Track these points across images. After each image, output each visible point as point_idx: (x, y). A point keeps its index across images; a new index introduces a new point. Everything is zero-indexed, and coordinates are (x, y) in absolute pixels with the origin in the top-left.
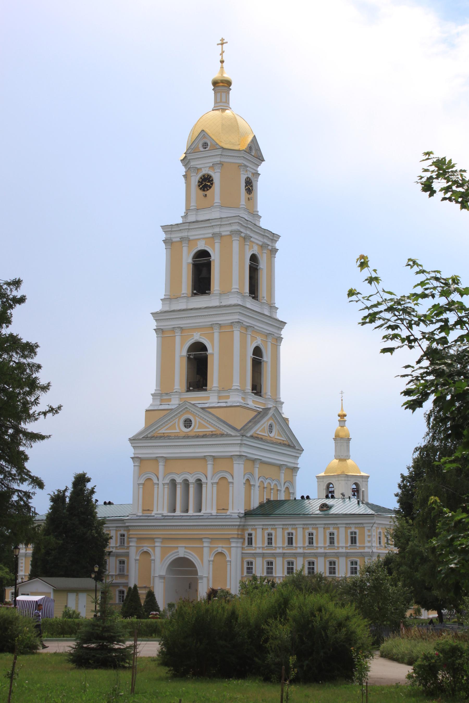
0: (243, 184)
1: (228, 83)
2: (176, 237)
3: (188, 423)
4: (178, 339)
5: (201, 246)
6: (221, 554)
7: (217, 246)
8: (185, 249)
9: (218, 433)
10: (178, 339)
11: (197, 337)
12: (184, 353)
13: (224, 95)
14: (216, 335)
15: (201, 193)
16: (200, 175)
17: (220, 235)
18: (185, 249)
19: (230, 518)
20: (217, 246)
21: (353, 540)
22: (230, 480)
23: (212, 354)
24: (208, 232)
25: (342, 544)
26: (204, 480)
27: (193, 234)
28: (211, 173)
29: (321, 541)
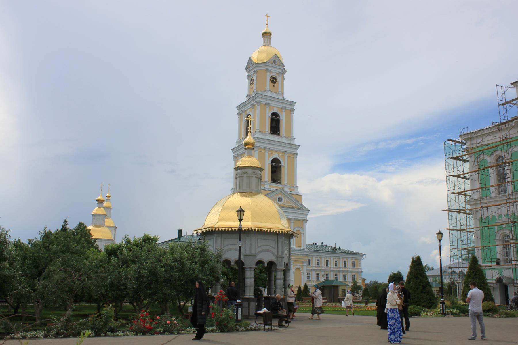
0: (255, 82)
1: (270, 34)
2: (264, 101)
4: (267, 154)
5: (276, 110)
6: (298, 269)
7: (284, 113)
8: (268, 109)
9: (296, 207)
10: (267, 154)
11: (276, 156)
12: (270, 162)
13: (268, 39)
16: (271, 75)
18: (268, 109)
19: (303, 250)
20: (284, 113)
21: (353, 265)
22: (302, 232)
23: (284, 166)
24: (280, 105)
25: (323, 265)
28: (277, 76)
29: (341, 265)
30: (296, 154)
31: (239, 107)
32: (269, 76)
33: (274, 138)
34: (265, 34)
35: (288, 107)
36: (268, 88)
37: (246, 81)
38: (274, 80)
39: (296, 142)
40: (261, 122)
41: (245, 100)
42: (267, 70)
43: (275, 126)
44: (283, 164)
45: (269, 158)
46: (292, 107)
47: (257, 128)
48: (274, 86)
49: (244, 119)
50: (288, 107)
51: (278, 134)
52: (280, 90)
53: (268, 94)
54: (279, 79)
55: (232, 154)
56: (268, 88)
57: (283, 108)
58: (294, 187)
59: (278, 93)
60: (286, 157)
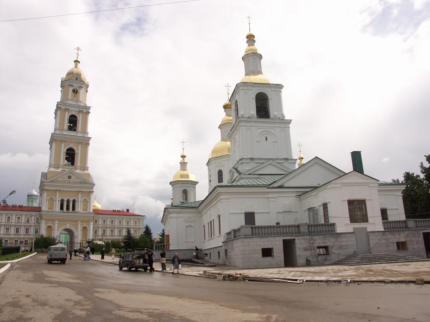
3: (70, 177)
4: (63, 145)
5: (74, 113)
7: (81, 115)
10: (63, 145)
11: (71, 146)
14: (80, 147)
15: (73, 95)
16: (73, 88)
17: (82, 111)
22: (88, 200)
23: (77, 153)
24: (78, 110)
26: (77, 200)
27: (70, 108)
28: (78, 89)
30: (88, 144)
32: (71, 89)
33: (72, 133)
35: (85, 111)
36: (70, 97)
39: (89, 136)
42: (70, 85)
44: (76, 152)
45: (64, 148)
46: (88, 110)
48: (75, 96)
51: (75, 130)
56: (70, 97)
57: (80, 112)
58: (84, 168)
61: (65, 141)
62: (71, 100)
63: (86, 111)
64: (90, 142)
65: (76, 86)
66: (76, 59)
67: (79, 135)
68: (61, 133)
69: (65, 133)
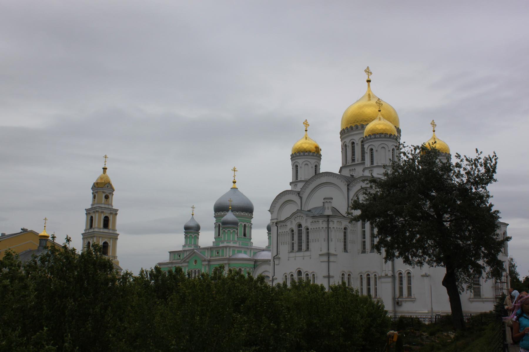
2: (100, 210)
4: (101, 240)
5: (107, 215)
7: (111, 216)
10: (101, 240)
11: (106, 240)
14: (111, 241)
24: (109, 212)
30: (117, 239)
31: (86, 210)
32: (104, 195)
33: (106, 231)
34: (103, 168)
35: (114, 213)
36: (103, 202)
37: (91, 196)
38: (107, 197)
39: (117, 232)
40: (98, 222)
41: (90, 207)
43: (106, 223)
47: (96, 226)
49: (89, 218)
50: (114, 213)
52: (110, 202)
53: (103, 206)
54: (110, 196)
55: (82, 237)
56: (103, 202)
57: (111, 213)
59: (109, 205)
60: (111, 241)
61: (102, 237)
62: (105, 204)
63: (115, 213)
64: (119, 237)
65: (107, 192)
66: (103, 166)
67: (111, 232)
68: (99, 230)
69: (102, 230)
